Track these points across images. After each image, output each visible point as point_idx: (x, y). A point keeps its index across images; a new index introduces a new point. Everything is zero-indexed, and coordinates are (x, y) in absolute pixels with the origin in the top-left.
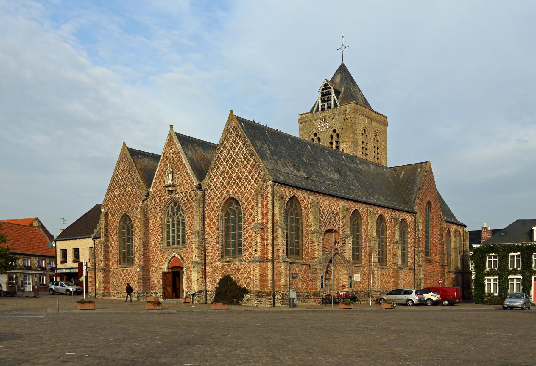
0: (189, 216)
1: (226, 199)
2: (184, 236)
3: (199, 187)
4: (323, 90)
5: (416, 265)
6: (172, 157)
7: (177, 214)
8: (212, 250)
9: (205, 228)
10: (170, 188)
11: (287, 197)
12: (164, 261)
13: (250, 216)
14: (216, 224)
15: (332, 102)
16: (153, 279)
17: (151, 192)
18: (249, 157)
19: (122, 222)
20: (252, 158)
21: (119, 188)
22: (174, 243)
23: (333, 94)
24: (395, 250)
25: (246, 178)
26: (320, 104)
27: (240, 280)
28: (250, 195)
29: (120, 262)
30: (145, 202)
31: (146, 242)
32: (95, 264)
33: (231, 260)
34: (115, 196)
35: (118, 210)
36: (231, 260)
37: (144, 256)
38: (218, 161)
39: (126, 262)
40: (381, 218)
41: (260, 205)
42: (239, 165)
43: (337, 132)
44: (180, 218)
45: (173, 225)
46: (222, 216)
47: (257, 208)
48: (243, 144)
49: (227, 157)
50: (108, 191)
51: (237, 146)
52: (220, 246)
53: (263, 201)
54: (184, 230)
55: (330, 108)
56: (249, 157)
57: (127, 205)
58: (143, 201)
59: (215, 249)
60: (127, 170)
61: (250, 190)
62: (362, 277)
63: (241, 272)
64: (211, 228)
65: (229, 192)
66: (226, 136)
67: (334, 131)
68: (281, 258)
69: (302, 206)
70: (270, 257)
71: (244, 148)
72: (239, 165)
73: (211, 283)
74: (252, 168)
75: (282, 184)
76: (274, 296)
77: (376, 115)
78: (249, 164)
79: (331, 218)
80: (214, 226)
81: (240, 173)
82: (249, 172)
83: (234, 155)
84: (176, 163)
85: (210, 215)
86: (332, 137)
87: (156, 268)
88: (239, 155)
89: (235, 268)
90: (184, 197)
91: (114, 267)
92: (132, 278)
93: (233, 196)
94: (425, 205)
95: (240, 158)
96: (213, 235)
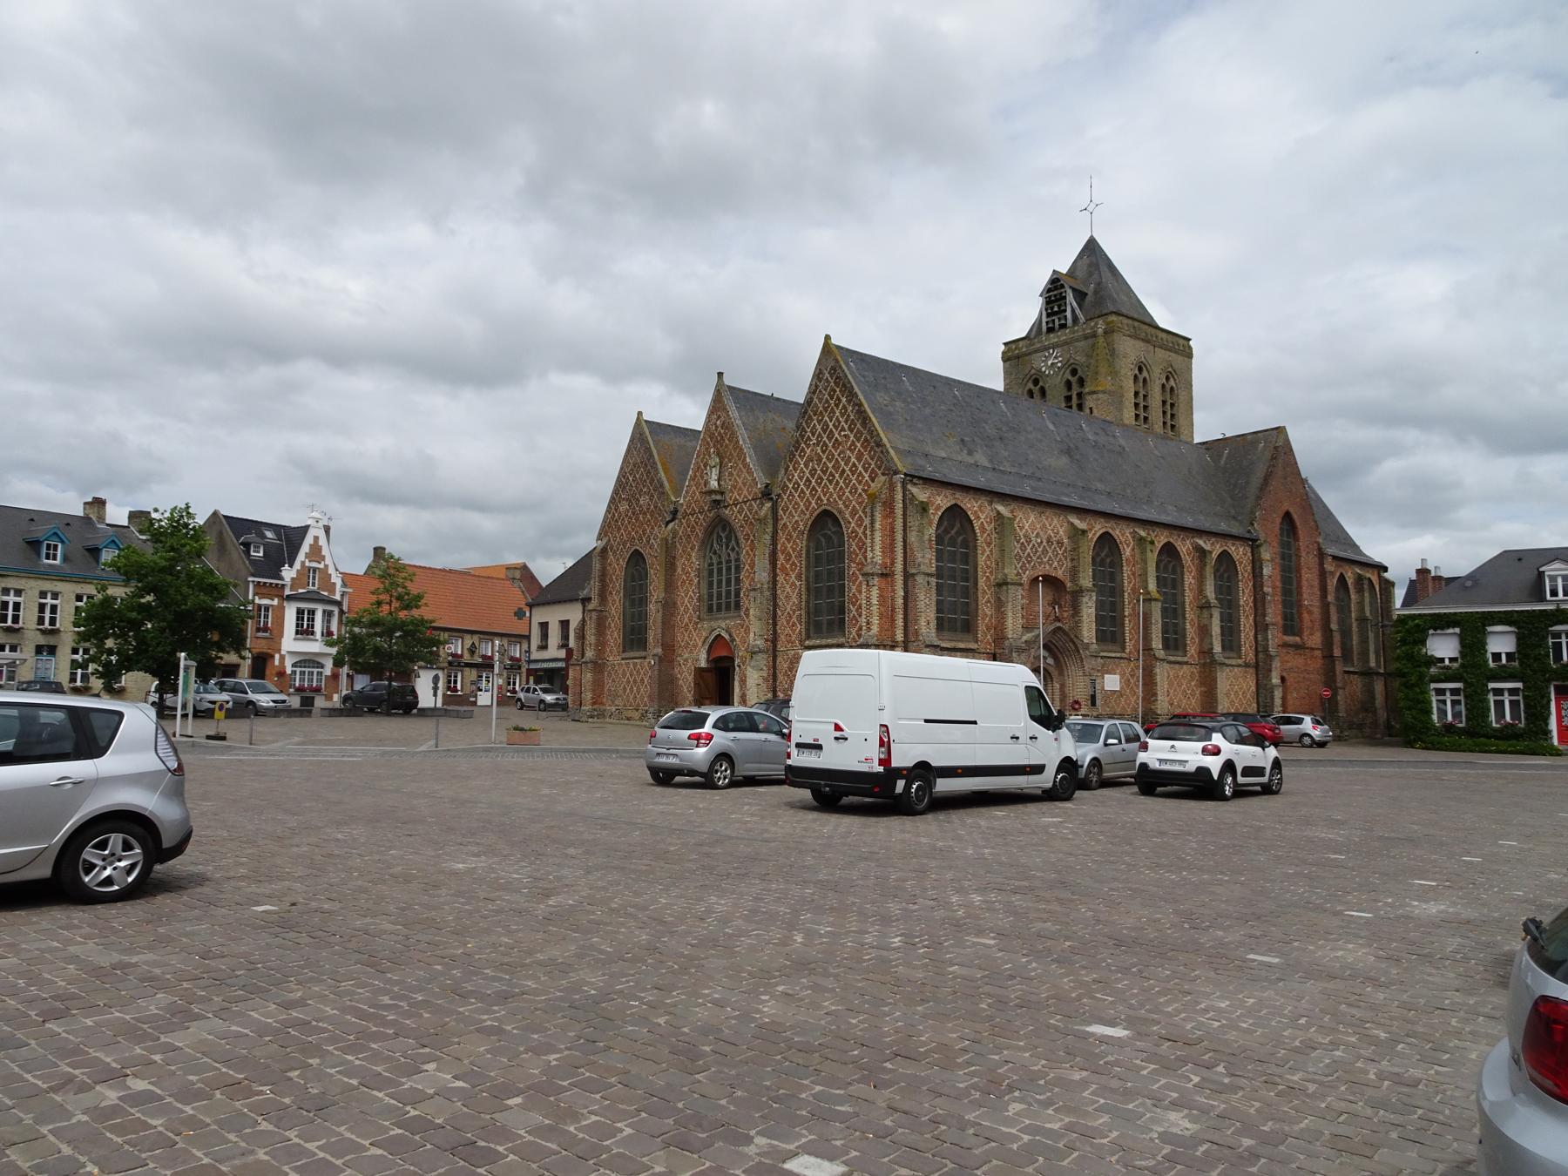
2: (737, 594)
3: (766, 494)
4: (1049, 290)
5: (1261, 655)
9: (775, 575)
10: (714, 497)
11: (938, 508)
15: (1069, 314)
22: (719, 609)
23: (1070, 297)
24: (1205, 621)
26: (1044, 319)
31: (669, 607)
37: (663, 635)
40: (1169, 551)
41: (877, 526)
43: (1080, 373)
46: (808, 552)
48: (849, 402)
49: (819, 428)
53: (885, 517)
54: (738, 580)
55: (1063, 326)
62: (1126, 682)
67: (1074, 372)
69: (976, 525)
75: (928, 481)
77: (1164, 335)
79: (1045, 551)
82: (859, 458)
86: (1069, 385)
91: (614, 658)
94: (1278, 520)
96: (792, 592)
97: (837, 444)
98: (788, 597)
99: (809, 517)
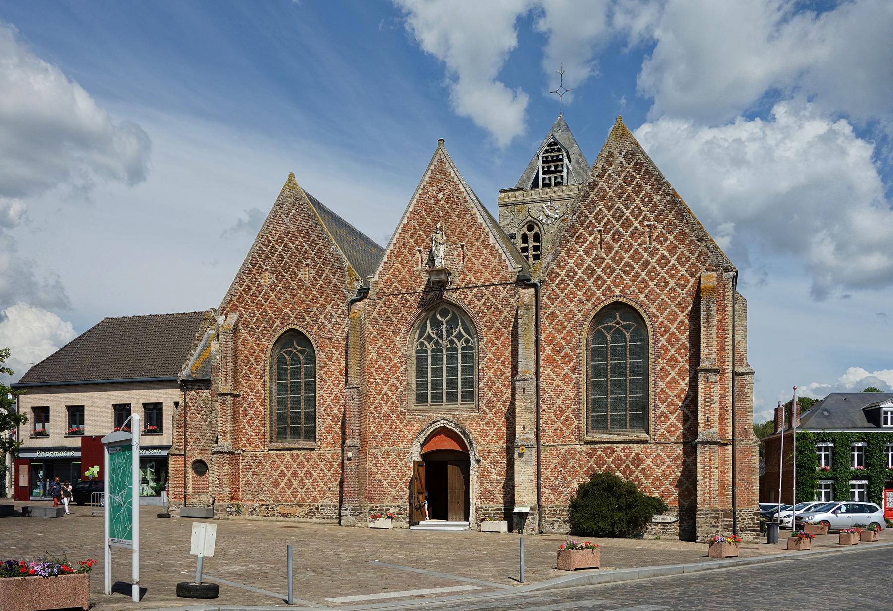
0: (490, 340)
1: (600, 307)
6: (442, 208)
8: (558, 417)
12: (410, 436)
13: (673, 345)
16: (378, 476)
17: (376, 283)
21: (273, 273)
22: (437, 398)
25: (663, 262)
28: (673, 299)
30: (358, 305)
32: (186, 439)
34: (260, 288)
35: (270, 322)
36: (615, 438)
38: (581, 223)
39: (289, 436)
45: (437, 359)
47: (708, 327)
49: (608, 215)
50: (238, 276)
52: (583, 407)
57: (301, 309)
58: (353, 301)
59: (568, 413)
61: (673, 289)
63: (644, 466)
65: (612, 292)
70: (730, 436)
73: (555, 490)
74: (682, 242)
76: (734, 519)
78: (671, 232)
81: (646, 250)
82: (672, 250)
83: (627, 213)
85: (554, 339)
87: (388, 453)
89: (627, 456)
92: (309, 474)
93: (625, 300)
97: (636, 234)
98: (558, 390)
99: (592, 309)
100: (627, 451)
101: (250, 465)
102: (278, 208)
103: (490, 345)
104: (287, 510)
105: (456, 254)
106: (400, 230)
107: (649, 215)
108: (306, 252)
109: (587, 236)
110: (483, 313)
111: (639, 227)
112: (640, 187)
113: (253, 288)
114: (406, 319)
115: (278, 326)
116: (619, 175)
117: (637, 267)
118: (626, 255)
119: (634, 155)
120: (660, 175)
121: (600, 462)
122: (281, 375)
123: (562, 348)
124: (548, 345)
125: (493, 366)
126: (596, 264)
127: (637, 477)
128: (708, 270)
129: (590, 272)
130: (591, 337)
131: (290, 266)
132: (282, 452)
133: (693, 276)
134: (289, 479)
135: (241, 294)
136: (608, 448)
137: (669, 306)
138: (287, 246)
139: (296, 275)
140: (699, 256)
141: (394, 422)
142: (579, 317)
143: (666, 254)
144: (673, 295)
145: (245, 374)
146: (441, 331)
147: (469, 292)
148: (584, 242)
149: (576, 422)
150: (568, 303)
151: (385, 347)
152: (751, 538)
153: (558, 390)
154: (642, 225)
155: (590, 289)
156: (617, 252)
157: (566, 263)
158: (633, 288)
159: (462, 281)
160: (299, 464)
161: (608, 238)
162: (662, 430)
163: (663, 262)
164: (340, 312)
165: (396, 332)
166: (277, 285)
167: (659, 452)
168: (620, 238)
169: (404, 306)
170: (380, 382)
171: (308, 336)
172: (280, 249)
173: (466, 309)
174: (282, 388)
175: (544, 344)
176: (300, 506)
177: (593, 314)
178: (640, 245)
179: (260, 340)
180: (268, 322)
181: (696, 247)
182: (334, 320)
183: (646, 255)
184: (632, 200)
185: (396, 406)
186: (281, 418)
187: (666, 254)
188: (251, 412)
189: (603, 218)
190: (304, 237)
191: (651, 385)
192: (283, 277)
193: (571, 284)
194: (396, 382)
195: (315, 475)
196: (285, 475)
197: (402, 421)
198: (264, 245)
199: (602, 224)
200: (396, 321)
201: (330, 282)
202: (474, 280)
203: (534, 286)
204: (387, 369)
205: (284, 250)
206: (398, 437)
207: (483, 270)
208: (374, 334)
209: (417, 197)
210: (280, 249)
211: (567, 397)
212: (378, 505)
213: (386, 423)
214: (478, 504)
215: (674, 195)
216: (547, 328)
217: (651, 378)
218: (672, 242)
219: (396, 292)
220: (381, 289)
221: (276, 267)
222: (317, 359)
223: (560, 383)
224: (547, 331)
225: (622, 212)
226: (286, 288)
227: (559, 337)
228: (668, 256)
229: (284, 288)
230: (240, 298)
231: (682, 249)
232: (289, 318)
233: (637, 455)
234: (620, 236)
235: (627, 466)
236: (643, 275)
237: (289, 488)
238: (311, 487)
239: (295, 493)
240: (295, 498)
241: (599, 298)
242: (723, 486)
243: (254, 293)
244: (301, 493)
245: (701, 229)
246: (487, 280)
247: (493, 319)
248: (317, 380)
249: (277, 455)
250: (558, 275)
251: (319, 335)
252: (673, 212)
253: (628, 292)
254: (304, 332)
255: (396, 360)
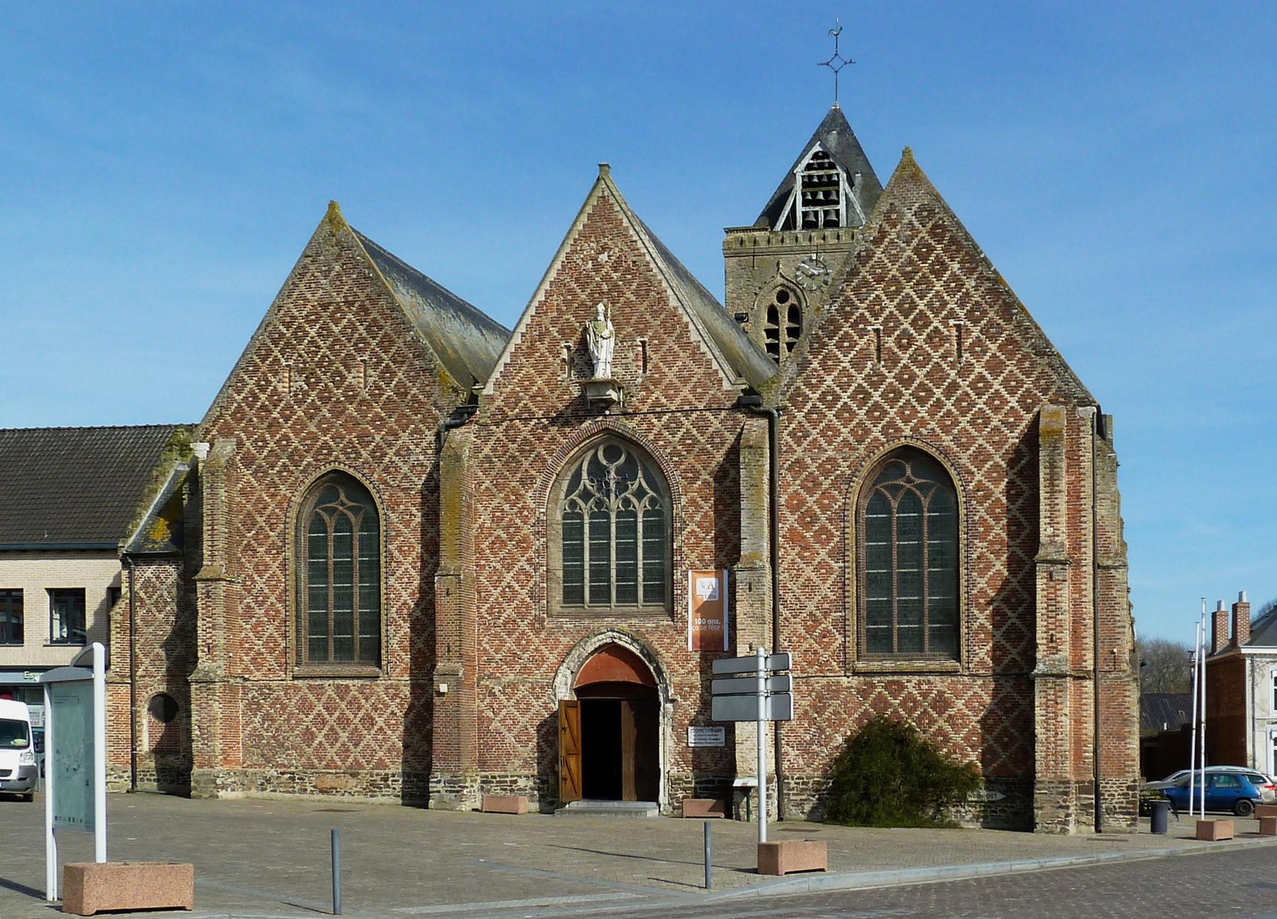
0: (693, 502)
3: (749, 403)
6: (607, 278)
7: (622, 487)
8: (809, 630)
12: (552, 659)
14: (830, 536)
16: (495, 725)
17: (491, 399)
18: (991, 314)
19: (313, 500)
20: (1008, 320)
21: (300, 372)
22: (601, 595)
25: (980, 386)
27: (947, 739)
29: (298, 654)
30: (457, 434)
32: (133, 657)
33: (904, 665)
34: (276, 398)
36: (904, 665)
38: (847, 317)
42: (944, 339)
44: (640, 507)
45: (600, 530)
49: (891, 307)
51: (938, 275)
56: (991, 314)
58: (448, 427)
59: (827, 624)
60: (349, 304)
61: (996, 429)
63: (952, 712)
64: (806, 548)
65: (898, 430)
66: (883, 234)
68: (1125, 666)
71: (970, 283)
72: (944, 339)
73: (805, 749)
74: (1010, 356)
78: (993, 339)
80: (824, 544)
82: (995, 367)
83: (921, 305)
84: (628, 303)
85: (802, 502)
87: (513, 686)
88: (944, 304)
90: (670, 428)
92: (369, 721)
93: (918, 444)
95: (952, 315)
97: (936, 338)
100: (925, 687)
101: (258, 703)
102: (308, 260)
103: (691, 509)
104: (329, 781)
105: (631, 355)
106: (532, 311)
107: (957, 310)
108: (362, 340)
109: (856, 338)
110: (679, 455)
111: (941, 327)
112: (942, 263)
113: (263, 397)
114: (545, 460)
115: (309, 464)
116: (908, 243)
117: (938, 393)
118: (921, 373)
119: (931, 213)
120: (975, 247)
121: (880, 702)
122: (316, 547)
123: (815, 519)
124: (793, 513)
125: (698, 544)
126: (872, 384)
127: (940, 728)
128: (1051, 402)
129: (862, 396)
130: (865, 503)
131: (331, 363)
132: (319, 682)
133: (1028, 410)
134: (332, 729)
135: (240, 406)
136: (893, 682)
137: (990, 457)
138: (325, 327)
139: (343, 378)
140: (1038, 379)
141: (523, 633)
142: (844, 467)
143: (985, 373)
144: (996, 439)
145: (249, 545)
146: (608, 484)
147: (655, 421)
148: (852, 347)
149: (840, 639)
150: (825, 445)
151: (507, 507)
152: (1124, 824)
153: (808, 586)
154: (947, 326)
155: (860, 424)
156: (905, 366)
157: (822, 380)
158: (933, 425)
159: (643, 401)
160: (350, 703)
161: (890, 342)
162: (981, 655)
163: (980, 386)
164: (424, 444)
165: (526, 481)
166: (306, 394)
167: (977, 689)
168: (910, 344)
169: (540, 439)
170: (499, 566)
171: (366, 483)
172: (313, 333)
173: (650, 448)
174: (318, 572)
175: (784, 511)
176: (354, 775)
177: (867, 465)
178: (944, 357)
179: (276, 487)
180: (290, 457)
181: (1033, 364)
182: (413, 458)
183: (953, 373)
184: (930, 285)
185: (528, 607)
186: (317, 624)
187: (985, 373)
188: (260, 612)
189: (882, 309)
190: (356, 314)
191: (963, 582)
192: (319, 380)
193: (830, 415)
194: (527, 567)
195: (380, 722)
196: (324, 722)
197: (537, 633)
198: (283, 323)
199: (881, 319)
200: (526, 464)
201: (406, 394)
202: (664, 400)
203: (768, 415)
204: (510, 545)
205: (320, 335)
206: (532, 660)
207: (679, 384)
208: (487, 484)
209: (562, 257)
210: (313, 333)
211: (826, 597)
212: (496, 774)
213: (509, 634)
214: (674, 771)
215: (997, 280)
216: (790, 486)
217: (963, 571)
218: (994, 355)
219: (525, 416)
220: (498, 408)
221: (305, 362)
222: (382, 523)
223: (813, 576)
224: (791, 490)
225: (913, 302)
226: (325, 400)
227: (811, 500)
228: (988, 376)
229: (320, 399)
230: (239, 415)
231: (1011, 367)
232: (331, 451)
233: (941, 693)
234: (911, 340)
235: (925, 711)
236: (949, 405)
237: (332, 745)
238: (373, 744)
239: (345, 751)
240: (343, 761)
241: (876, 439)
242: (1078, 743)
243: (263, 406)
244: (355, 753)
245: (1041, 336)
246: (685, 401)
247: (698, 466)
248: (383, 560)
249: (310, 687)
250: (807, 399)
251: (385, 483)
252: (996, 307)
253: (924, 432)
254: (358, 476)
255: (526, 530)
